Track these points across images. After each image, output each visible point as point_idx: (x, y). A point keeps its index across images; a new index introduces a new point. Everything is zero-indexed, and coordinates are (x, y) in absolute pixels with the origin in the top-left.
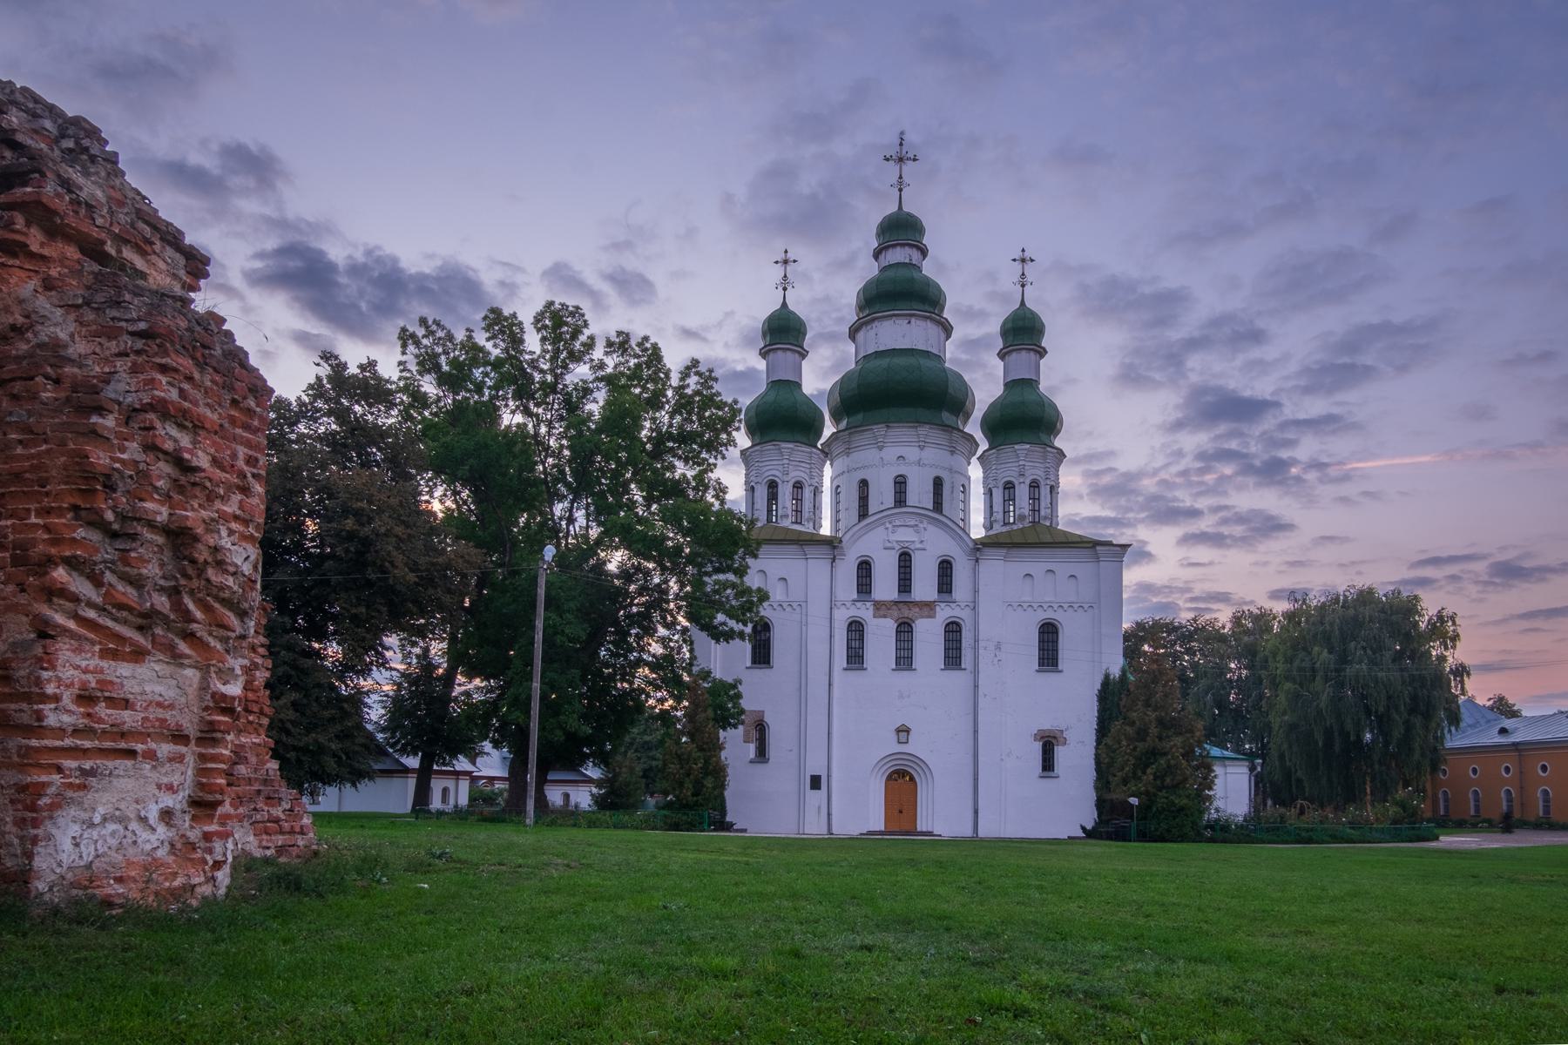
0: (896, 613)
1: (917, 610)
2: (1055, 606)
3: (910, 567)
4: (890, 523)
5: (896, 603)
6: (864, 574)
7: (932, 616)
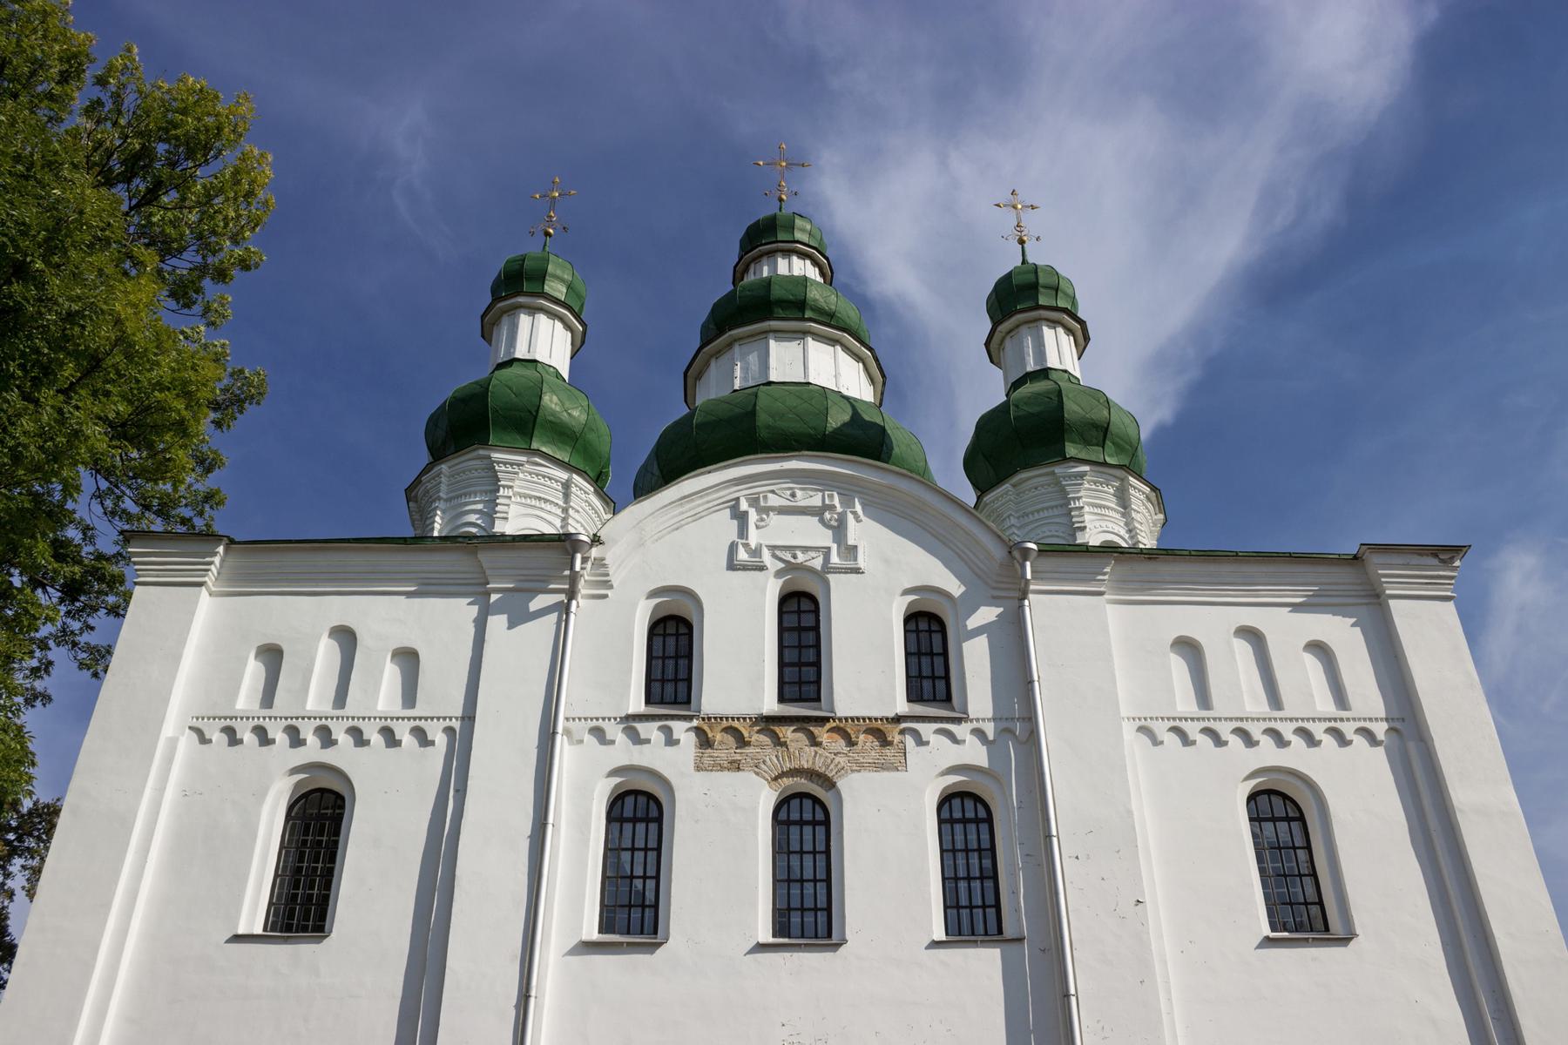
0: (773, 759)
1: (840, 744)
2: (1287, 730)
3: (816, 628)
4: (754, 502)
5: (768, 723)
6: (671, 650)
7: (899, 764)
